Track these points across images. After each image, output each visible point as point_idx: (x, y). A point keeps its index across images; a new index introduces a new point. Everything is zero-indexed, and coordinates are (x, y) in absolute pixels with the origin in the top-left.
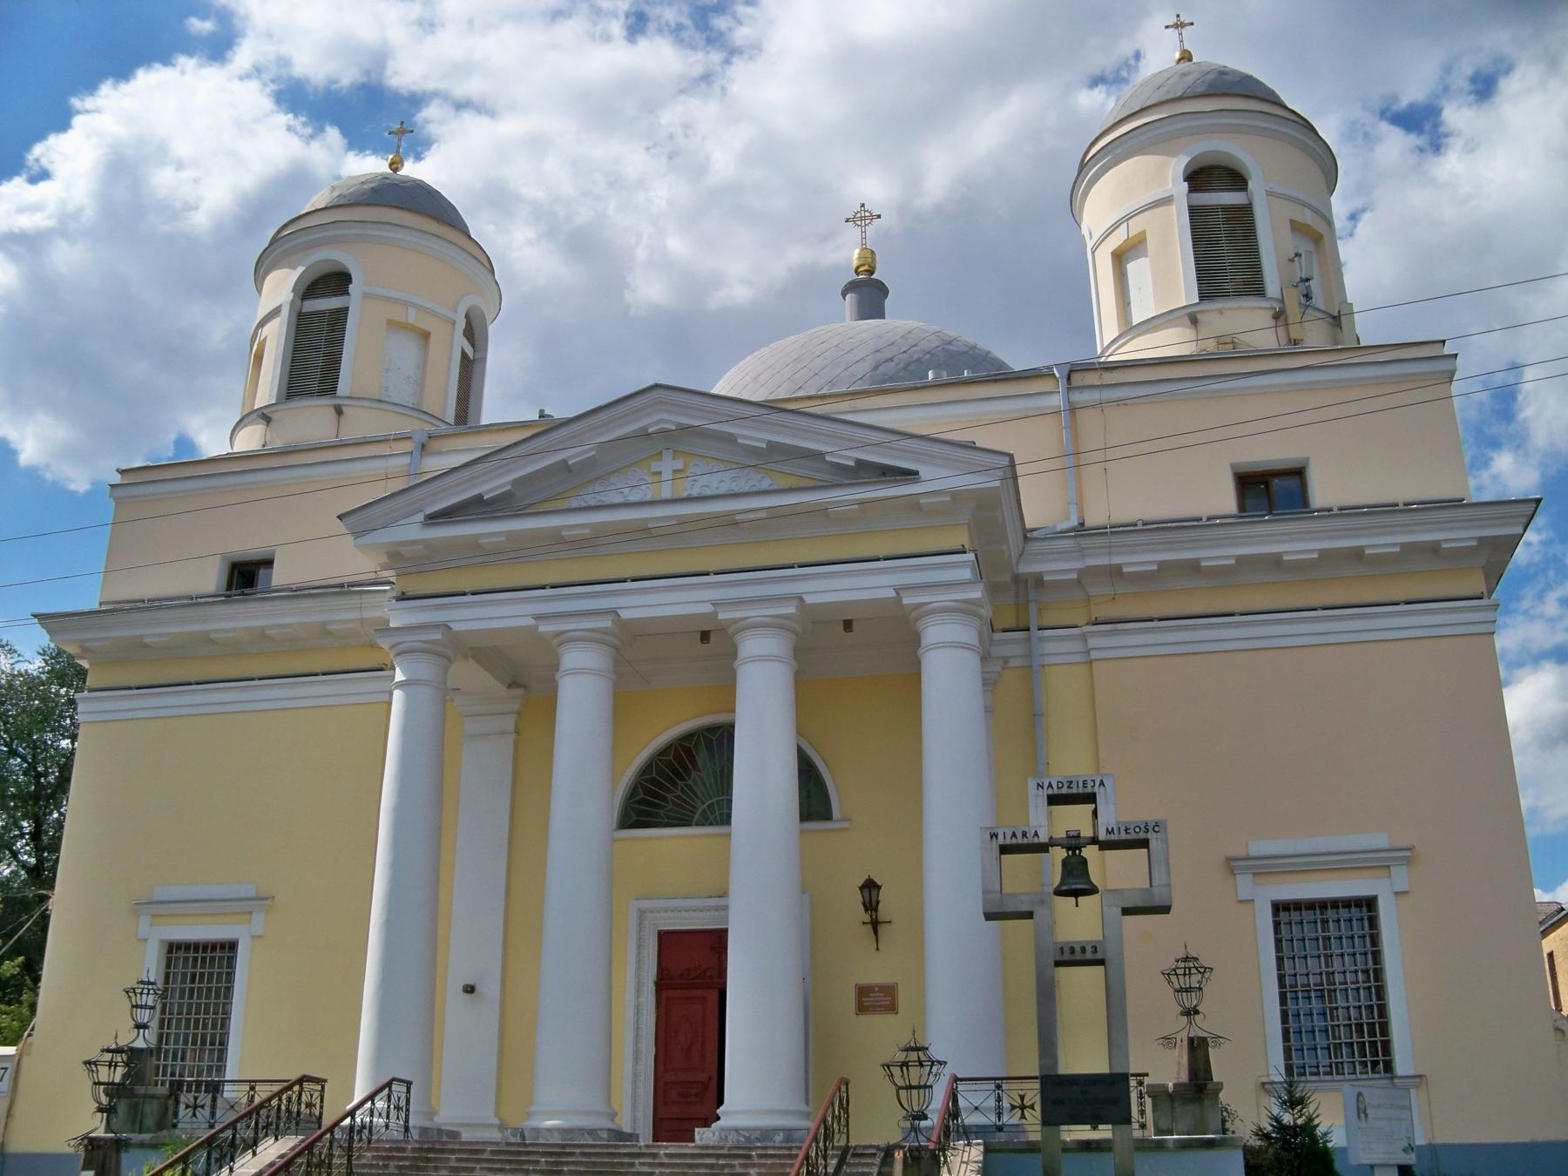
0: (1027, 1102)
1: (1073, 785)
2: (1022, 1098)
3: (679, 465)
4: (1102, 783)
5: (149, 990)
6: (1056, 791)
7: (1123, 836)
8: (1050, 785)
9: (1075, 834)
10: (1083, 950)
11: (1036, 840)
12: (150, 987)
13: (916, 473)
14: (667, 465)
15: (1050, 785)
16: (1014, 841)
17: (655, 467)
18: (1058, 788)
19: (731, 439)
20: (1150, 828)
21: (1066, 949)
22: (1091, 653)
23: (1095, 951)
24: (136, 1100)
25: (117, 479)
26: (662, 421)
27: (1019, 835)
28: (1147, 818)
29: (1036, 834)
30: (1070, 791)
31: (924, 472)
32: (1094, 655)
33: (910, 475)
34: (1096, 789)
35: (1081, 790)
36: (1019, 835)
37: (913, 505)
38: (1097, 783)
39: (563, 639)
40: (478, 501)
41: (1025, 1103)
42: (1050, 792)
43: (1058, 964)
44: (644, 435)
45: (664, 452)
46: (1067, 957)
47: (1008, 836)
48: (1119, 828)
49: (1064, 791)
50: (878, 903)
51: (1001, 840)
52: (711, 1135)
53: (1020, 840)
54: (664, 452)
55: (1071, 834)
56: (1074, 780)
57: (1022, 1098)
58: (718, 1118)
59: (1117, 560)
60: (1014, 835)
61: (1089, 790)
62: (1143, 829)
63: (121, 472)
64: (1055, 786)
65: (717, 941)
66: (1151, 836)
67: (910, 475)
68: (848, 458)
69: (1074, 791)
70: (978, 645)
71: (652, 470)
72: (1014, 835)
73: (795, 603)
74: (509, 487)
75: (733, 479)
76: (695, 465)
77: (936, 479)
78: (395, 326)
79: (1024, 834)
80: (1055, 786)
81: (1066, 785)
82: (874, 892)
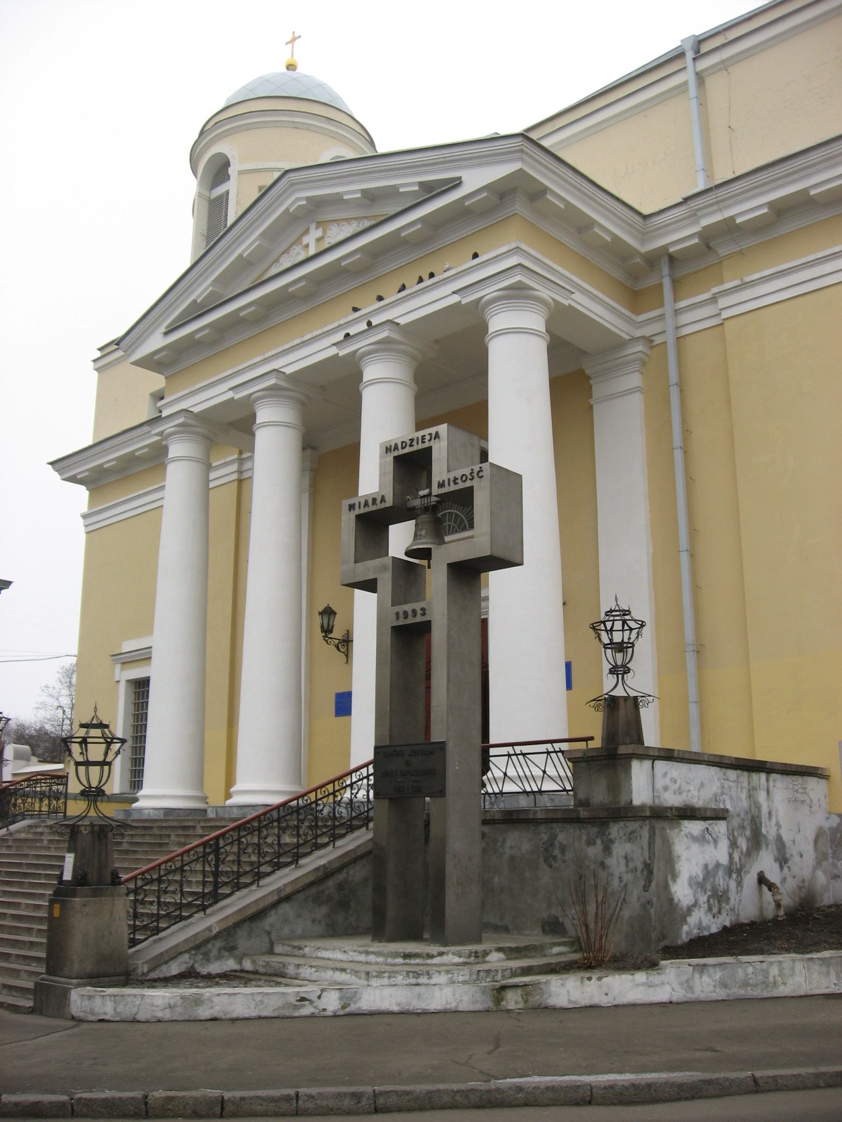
18: (403, 448)
25: (98, 354)
26: (298, 199)
32: (725, 314)
33: (456, 183)
34: (432, 443)
42: (396, 453)
51: (357, 511)
61: (426, 445)
62: (469, 477)
63: (100, 349)
67: (456, 183)
68: (409, 183)
70: (544, 331)
74: (211, 289)
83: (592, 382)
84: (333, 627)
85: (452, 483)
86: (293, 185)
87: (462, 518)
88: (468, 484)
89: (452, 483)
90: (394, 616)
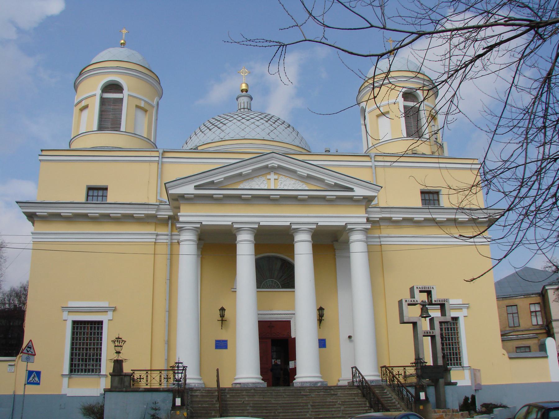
0: (400, 373)
1: (426, 288)
2: (398, 372)
3: (276, 177)
4: (433, 288)
5: (118, 340)
6: (421, 290)
7: (439, 302)
8: (420, 288)
9: (425, 301)
10: (427, 333)
11: (417, 303)
12: (120, 339)
13: (353, 189)
14: (272, 176)
15: (420, 288)
16: (411, 303)
17: (268, 177)
19: (294, 172)
20: (445, 300)
21: (426, 332)
22: (382, 242)
23: (433, 333)
24: (122, 376)
26: (273, 163)
27: (413, 301)
28: (444, 298)
29: (417, 301)
30: (425, 290)
31: (355, 188)
33: (351, 190)
34: (431, 290)
35: (428, 290)
36: (413, 301)
37: (350, 199)
38: (432, 288)
39: (239, 229)
40: (212, 182)
41: (399, 373)
42: (420, 290)
43: (424, 336)
44: (266, 167)
45: (271, 172)
46: (426, 334)
47: (410, 301)
48: (438, 301)
49: (423, 290)
50: (324, 314)
51: (408, 303)
52: (299, 384)
53: (413, 303)
54: (271, 172)
55: (423, 301)
56: (426, 287)
57: (398, 372)
58: (295, 379)
59: (392, 216)
60: (411, 301)
61: (429, 290)
64: (421, 288)
65: (286, 325)
66: (445, 303)
67: (351, 190)
68: (332, 181)
69: (426, 290)
71: (268, 178)
72: (411, 301)
73: (316, 224)
75: (294, 184)
76: (281, 178)
77: (359, 192)
78: (138, 107)
79: (414, 301)
80: (421, 288)
81: (424, 288)
82: (323, 310)
83: (336, 250)
84: (224, 315)
85: (438, 301)
86: (273, 157)
87: (278, 283)
88: (443, 302)
89: (438, 301)
90: (424, 333)
